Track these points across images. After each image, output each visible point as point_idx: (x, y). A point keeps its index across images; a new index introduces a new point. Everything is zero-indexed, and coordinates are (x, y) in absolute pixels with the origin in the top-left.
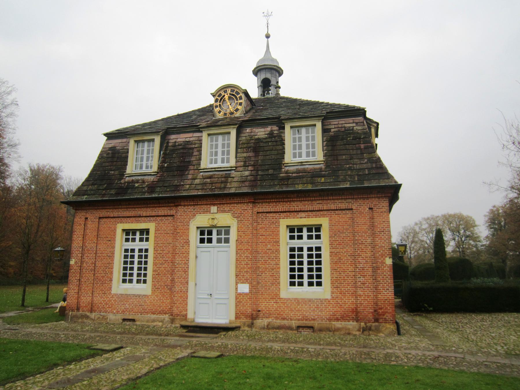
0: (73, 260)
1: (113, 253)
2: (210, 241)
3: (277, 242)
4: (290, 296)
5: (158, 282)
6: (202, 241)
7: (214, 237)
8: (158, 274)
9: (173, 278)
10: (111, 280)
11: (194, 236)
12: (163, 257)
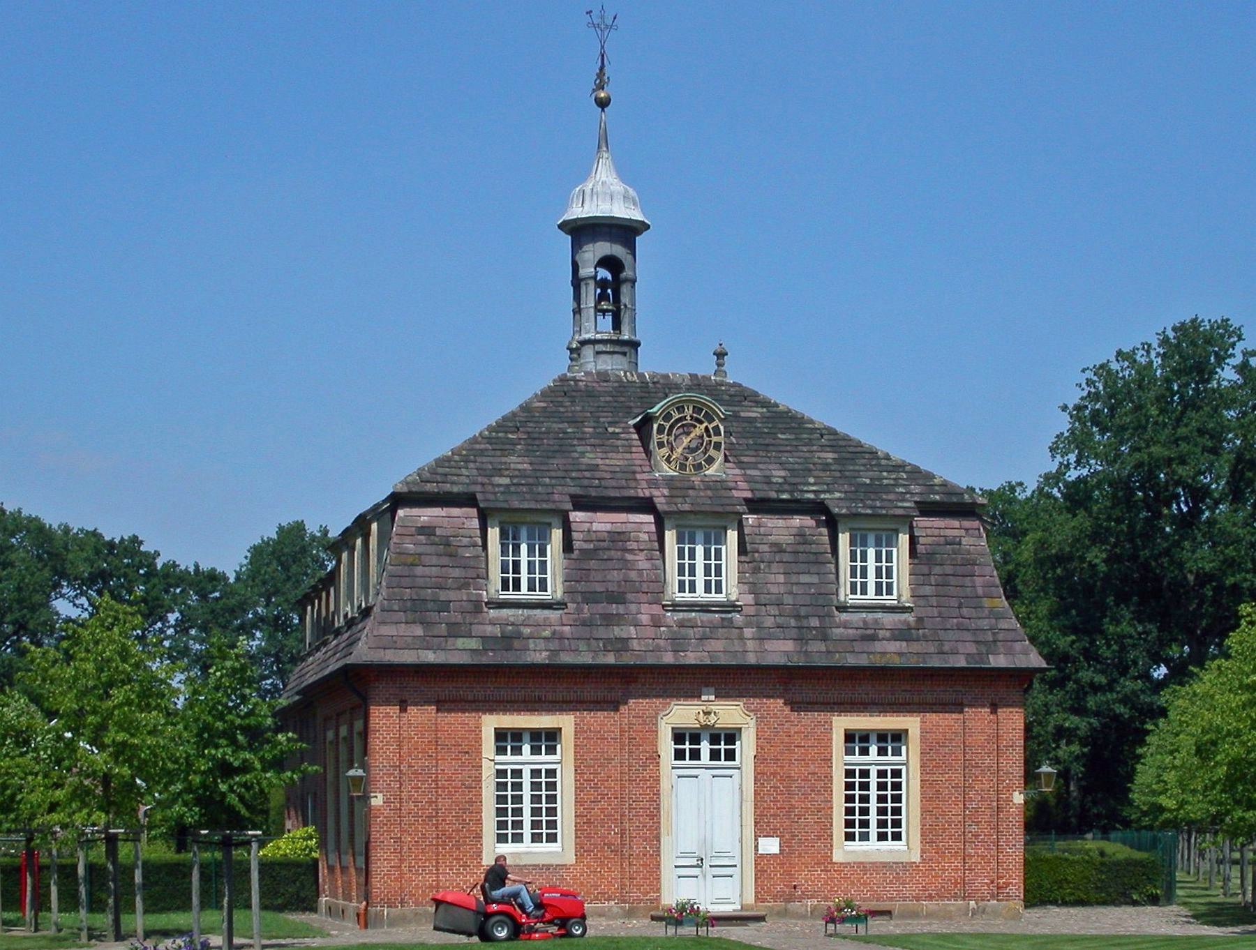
0: (380, 796)
1: (479, 780)
2: (695, 755)
3: (828, 761)
4: (850, 859)
5: (589, 837)
6: (679, 755)
7: (705, 747)
8: (589, 822)
9: (625, 825)
10: (479, 837)
11: (667, 747)
12: (596, 787)
